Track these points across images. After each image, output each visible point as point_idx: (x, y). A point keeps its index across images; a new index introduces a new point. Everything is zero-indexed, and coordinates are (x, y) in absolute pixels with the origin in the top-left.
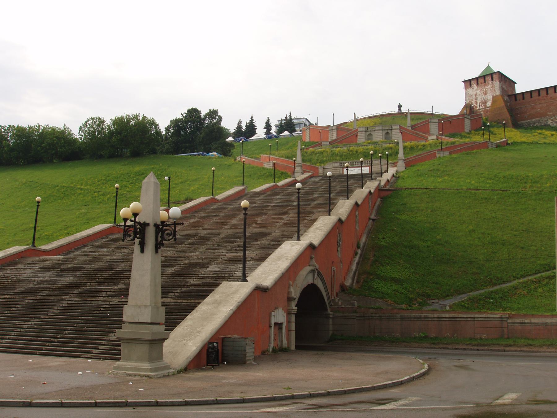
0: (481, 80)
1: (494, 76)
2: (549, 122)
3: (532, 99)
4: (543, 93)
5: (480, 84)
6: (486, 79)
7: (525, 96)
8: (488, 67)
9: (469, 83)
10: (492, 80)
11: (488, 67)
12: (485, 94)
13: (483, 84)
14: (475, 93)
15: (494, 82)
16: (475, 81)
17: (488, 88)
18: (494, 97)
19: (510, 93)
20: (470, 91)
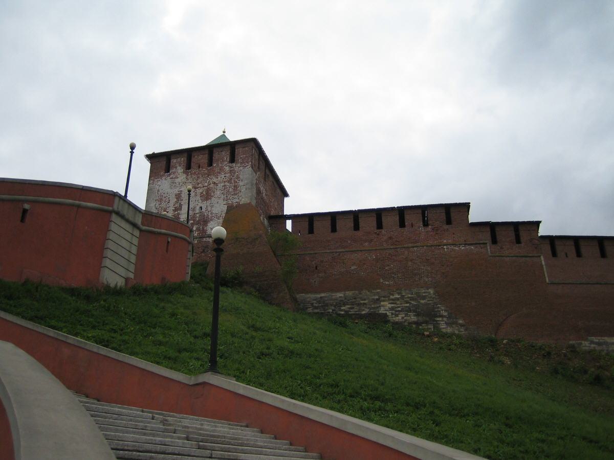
0: (203, 159)
1: (239, 150)
2: (385, 307)
3: (335, 235)
4: (368, 225)
5: (194, 170)
6: (216, 156)
7: (317, 224)
8: (223, 136)
9: (163, 163)
10: (233, 160)
11: (223, 136)
12: (207, 196)
13: (205, 170)
14: (176, 191)
15: (236, 167)
16: (183, 159)
17: (220, 180)
18: (230, 208)
19: (273, 213)
20: (164, 184)
